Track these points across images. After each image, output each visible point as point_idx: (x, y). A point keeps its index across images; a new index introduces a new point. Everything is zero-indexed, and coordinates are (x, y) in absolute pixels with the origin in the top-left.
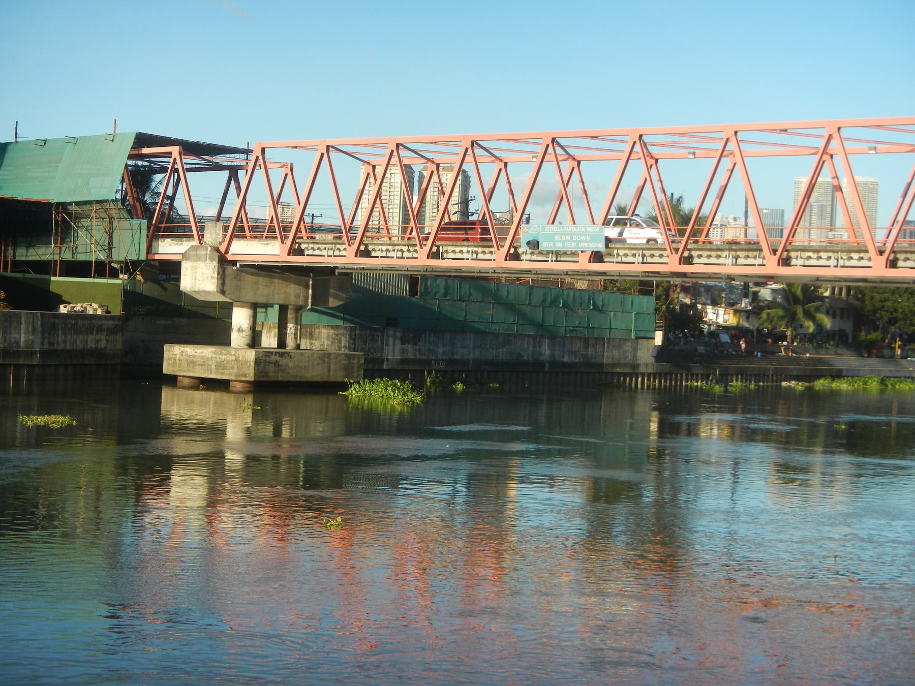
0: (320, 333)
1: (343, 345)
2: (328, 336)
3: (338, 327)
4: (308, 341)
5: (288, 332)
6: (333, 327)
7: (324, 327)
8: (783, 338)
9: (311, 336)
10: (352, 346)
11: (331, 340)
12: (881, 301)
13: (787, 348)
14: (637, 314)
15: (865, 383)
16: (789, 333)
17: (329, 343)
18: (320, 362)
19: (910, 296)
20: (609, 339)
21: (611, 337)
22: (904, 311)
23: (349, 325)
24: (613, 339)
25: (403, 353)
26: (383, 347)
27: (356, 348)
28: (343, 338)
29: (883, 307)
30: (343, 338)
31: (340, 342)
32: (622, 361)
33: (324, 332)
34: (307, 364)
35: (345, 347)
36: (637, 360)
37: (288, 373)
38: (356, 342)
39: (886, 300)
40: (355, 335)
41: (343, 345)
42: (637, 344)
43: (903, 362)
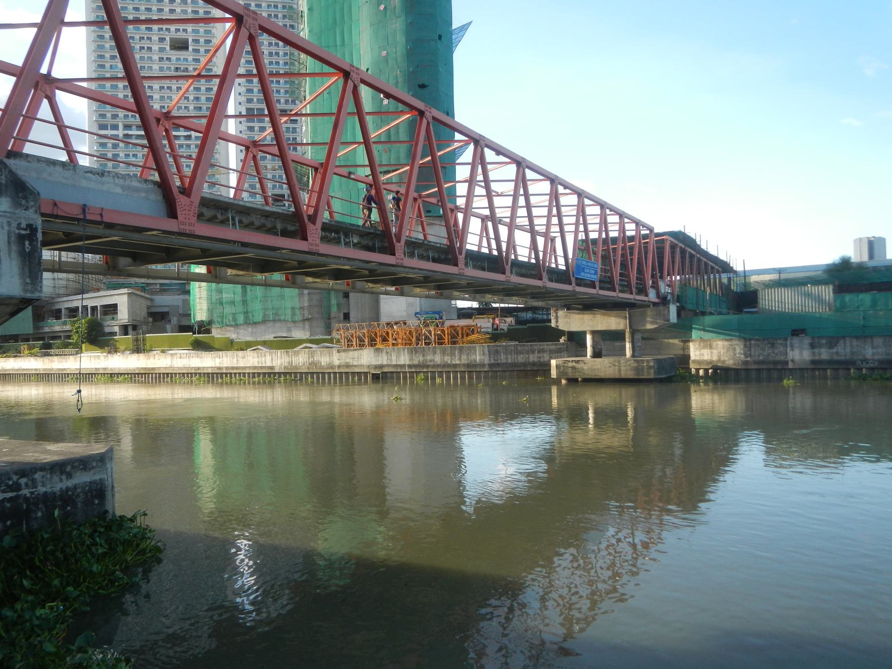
0: (717, 345)
2: (723, 346)
4: (709, 351)
6: (726, 340)
7: (720, 340)
9: (711, 347)
10: (749, 352)
17: (724, 351)
18: (611, 365)
25: (813, 356)
26: (787, 352)
27: (753, 354)
28: (737, 347)
30: (737, 347)
31: (735, 349)
33: (720, 343)
34: (600, 367)
37: (584, 373)
38: (753, 349)
40: (750, 344)
41: (738, 351)
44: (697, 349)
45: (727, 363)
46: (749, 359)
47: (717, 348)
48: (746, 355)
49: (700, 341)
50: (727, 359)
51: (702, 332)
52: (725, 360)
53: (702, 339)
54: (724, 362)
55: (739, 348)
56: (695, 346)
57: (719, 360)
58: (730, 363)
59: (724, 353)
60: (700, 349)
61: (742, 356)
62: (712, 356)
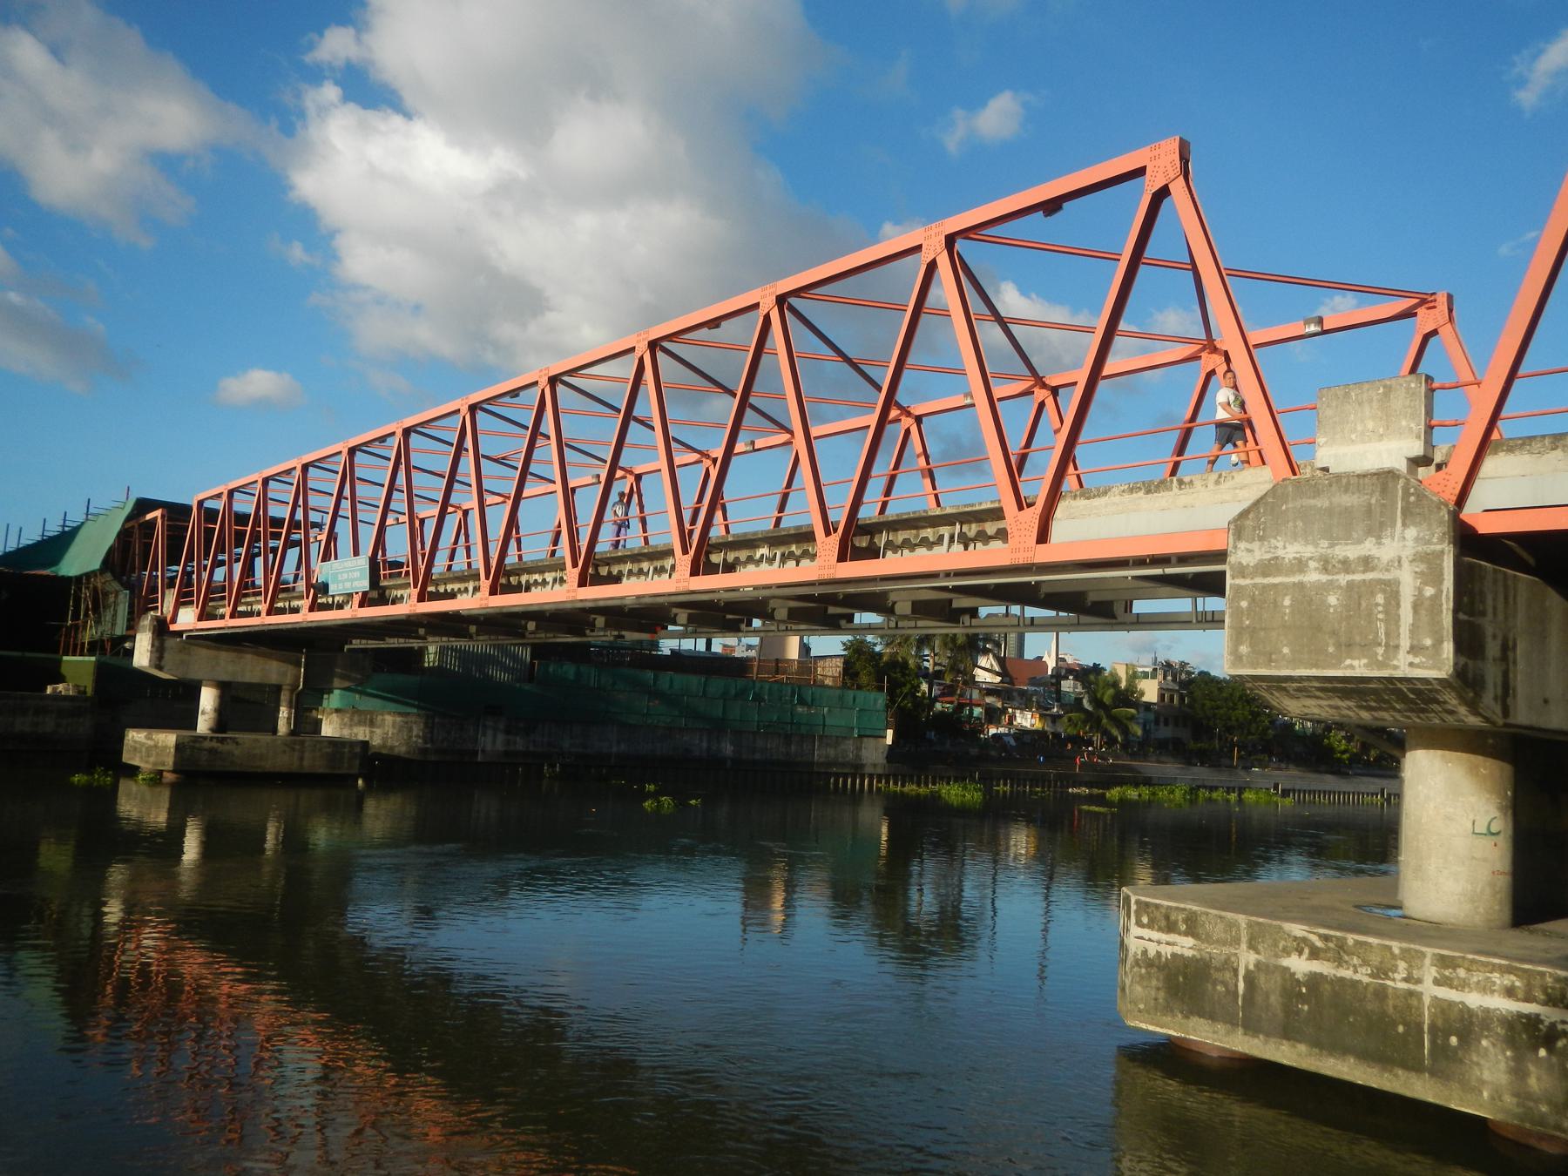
1: (415, 733)
2: (394, 724)
3: (409, 714)
4: (367, 730)
5: (280, 715)
6: (400, 714)
7: (389, 713)
8: (1090, 743)
9: (372, 724)
11: (397, 727)
12: (1212, 708)
13: (1090, 753)
14: (861, 710)
15: (1172, 792)
16: (1095, 739)
17: (395, 731)
19: (1245, 704)
20: (821, 737)
21: (826, 734)
22: (1237, 720)
23: (424, 712)
24: (826, 736)
29: (1215, 715)
32: (840, 760)
35: (418, 736)
36: (861, 759)
38: (436, 731)
39: (1218, 708)
41: (415, 733)
42: (861, 743)
43: (1242, 773)
44: (345, 725)
45: (396, 751)
46: (429, 746)
47: (382, 726)
48: (426, 742)
49: (353, 713)
50: (397, 744)
51: (357, 696)
52: (396, 746)
53: (355, 711)
54: (392, 748)
55: (417, 730)
56: (343, 719)
57: (384, 746)
58: (401, 750)
59: (393, 734)
60: (351, 726)
61: (420, 741)
62: (371, 738)
